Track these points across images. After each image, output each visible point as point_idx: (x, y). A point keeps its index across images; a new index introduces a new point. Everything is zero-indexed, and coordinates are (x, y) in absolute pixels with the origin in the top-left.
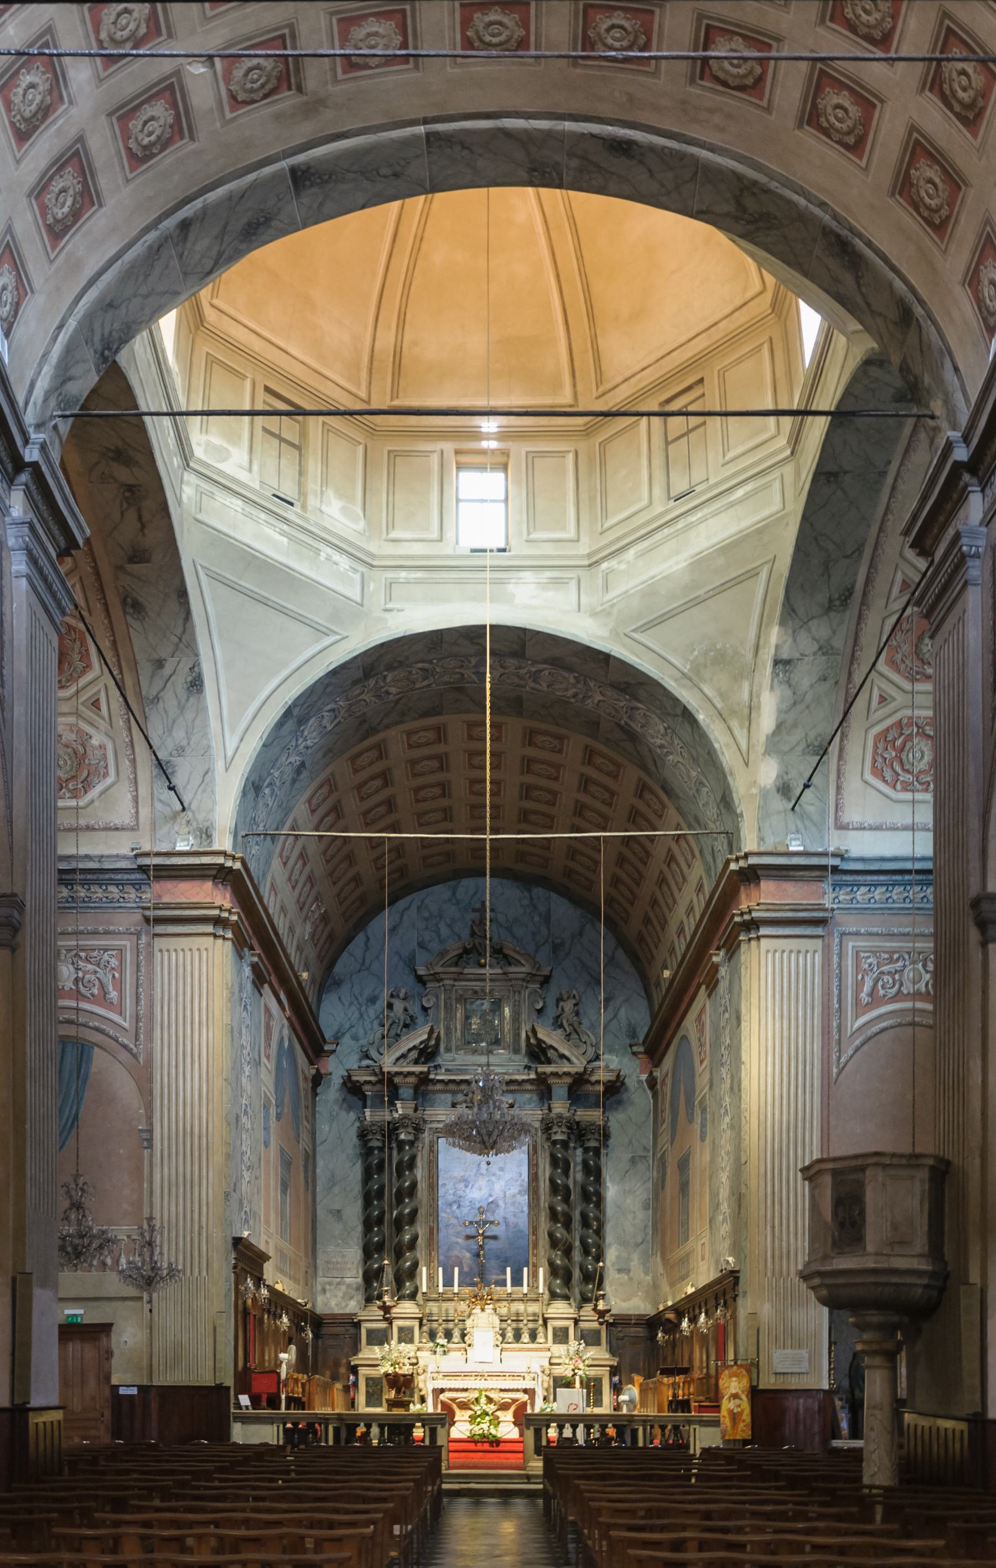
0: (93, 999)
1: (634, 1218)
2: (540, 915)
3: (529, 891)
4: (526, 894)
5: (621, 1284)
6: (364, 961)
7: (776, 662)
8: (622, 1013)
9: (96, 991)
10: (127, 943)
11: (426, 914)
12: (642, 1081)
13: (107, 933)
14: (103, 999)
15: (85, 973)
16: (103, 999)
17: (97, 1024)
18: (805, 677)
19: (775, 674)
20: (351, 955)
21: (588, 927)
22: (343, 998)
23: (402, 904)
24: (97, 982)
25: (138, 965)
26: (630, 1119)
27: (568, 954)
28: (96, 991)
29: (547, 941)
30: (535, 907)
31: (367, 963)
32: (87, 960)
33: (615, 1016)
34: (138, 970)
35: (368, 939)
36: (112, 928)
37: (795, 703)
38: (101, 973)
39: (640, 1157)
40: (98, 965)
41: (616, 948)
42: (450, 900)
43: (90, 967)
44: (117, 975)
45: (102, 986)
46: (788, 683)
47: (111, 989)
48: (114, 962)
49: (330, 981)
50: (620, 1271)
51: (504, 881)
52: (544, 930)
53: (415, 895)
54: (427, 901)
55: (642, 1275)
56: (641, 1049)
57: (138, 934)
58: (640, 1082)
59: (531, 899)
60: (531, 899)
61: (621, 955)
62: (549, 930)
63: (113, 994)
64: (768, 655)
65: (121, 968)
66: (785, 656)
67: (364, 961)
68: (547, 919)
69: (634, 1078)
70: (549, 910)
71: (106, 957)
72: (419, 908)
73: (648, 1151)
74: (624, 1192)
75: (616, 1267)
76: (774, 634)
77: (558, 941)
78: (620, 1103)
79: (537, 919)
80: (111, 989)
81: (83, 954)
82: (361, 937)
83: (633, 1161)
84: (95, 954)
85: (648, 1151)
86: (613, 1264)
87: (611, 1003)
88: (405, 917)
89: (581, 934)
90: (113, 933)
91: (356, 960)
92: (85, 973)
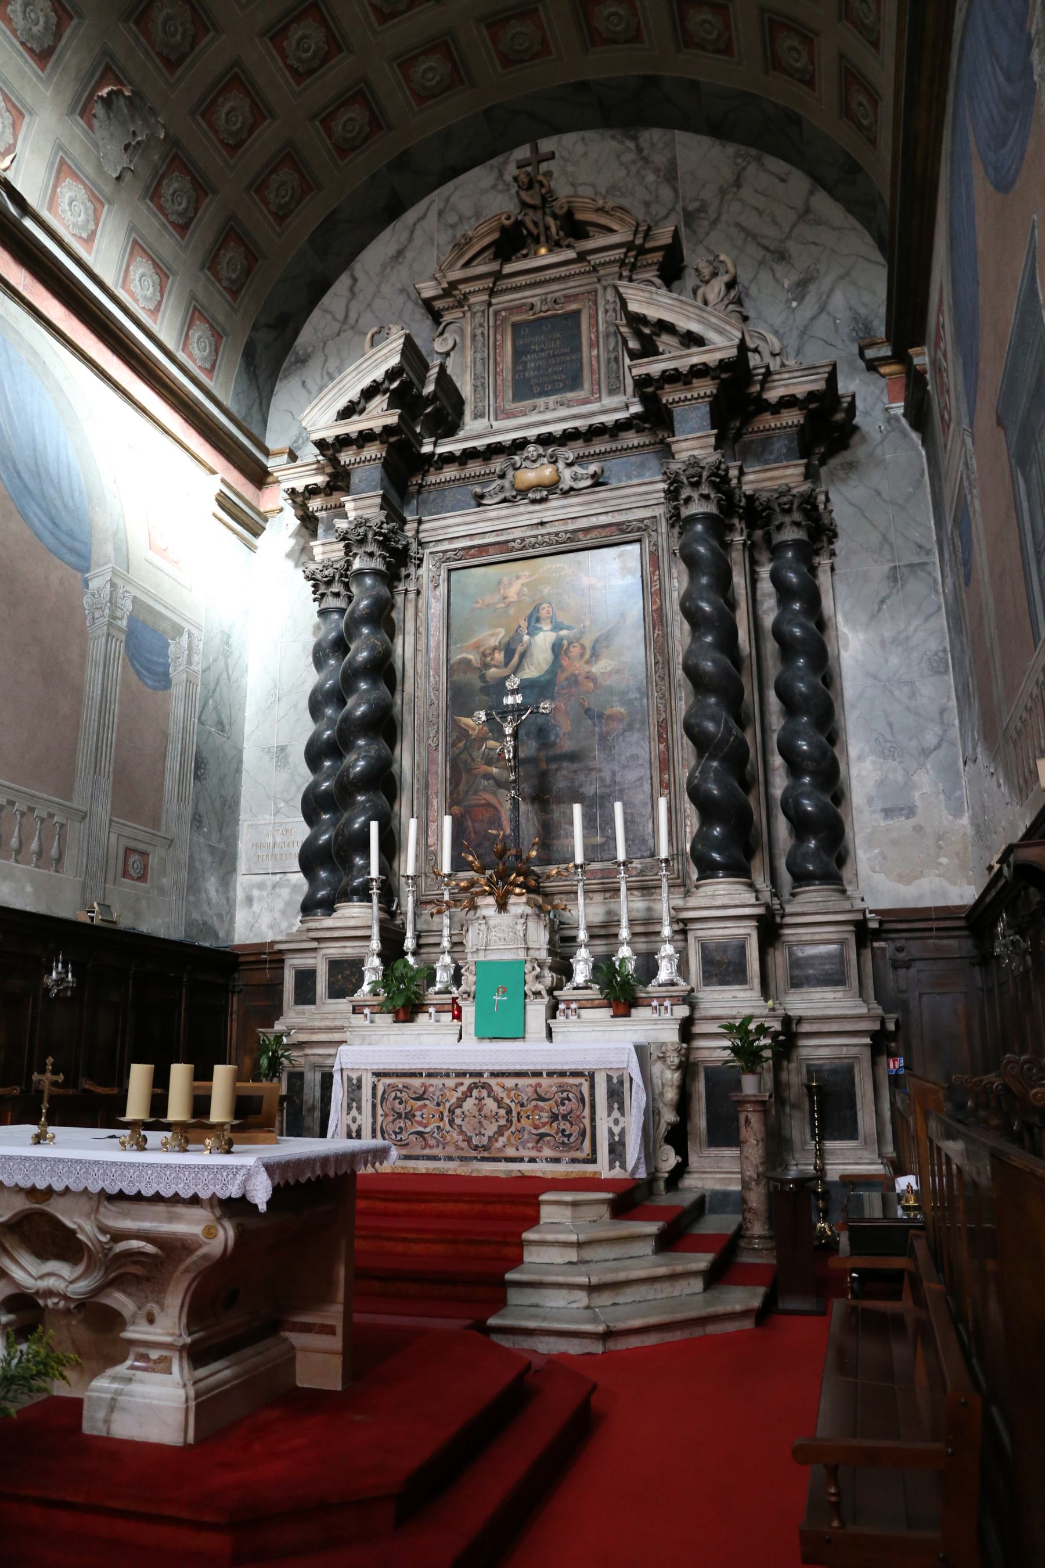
1: (913, 695)
2: (657, 171)
3: (635, 138)
4: (631, 145)
5: (894, 843)
6: (346, 317)
8: (838, 300)
11: (452, 218)
12: (896, 418)
20: (326, 311)
21: (752, 168)
22: (310, 383)
23: (410, 216)
26: (879, 494)
27: (717, 220)
29: (673, 209)
30: (646, 160)
31: (352, 320)
33: (822, 309)
35: (355, 280)
39: (911, 566)
41: (811, 193)
42: (494, 187)
49: (290, 358)
50: (888, 813)
51: (589, 134)
52: (666, 193)
53: (434, 195)
54: (453, 199)
55: (947, 818)
56: (886, 351)
58: (891, 420)
59: (639, 150)
60: (639, 150)
61: (823, 203)
62: (675, 190)
67: (346, 317)
68: (670, 176)
69: (878, 413)
70: (673, 162)
72: (440, 213)
73: (929, 552)
74: (883, 644)
75: (879, 805)
77: (693, 206)
78: (851, 466)
79: (651, 178)
82: (343, 282)
83: (894, 576)
85: (929, 552)
86: (870, 801)
87: (812, 288)
88: (418, 232)
89: (738, 184)
91: (335, 319)
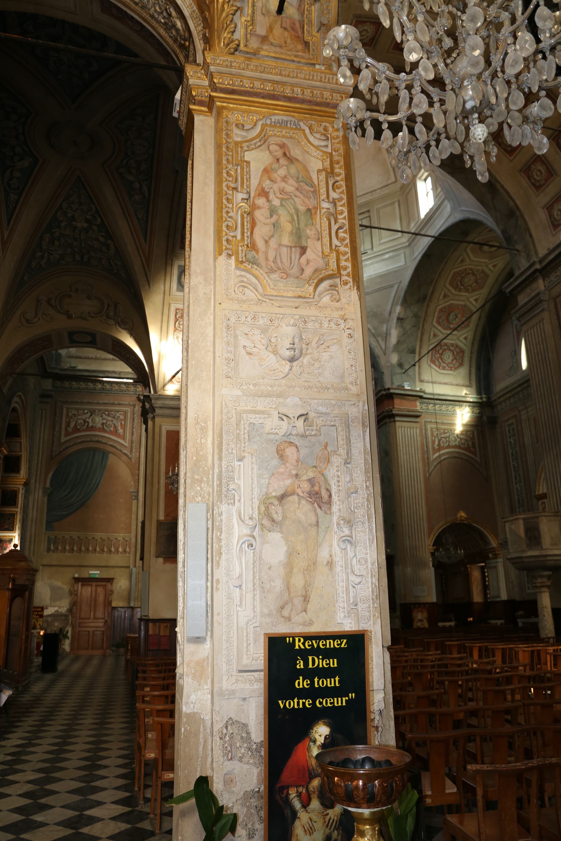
0: (111, 433)
7: (399, 319)
9: (112, 429)
10: (129, 409)
13: (119, 404)
14: (115, 433)
15: (107, 421)
16: (115, 433)
17: (112, 443)
18: (408, 325)
19: (397, 323)
24: (113, 425)
25: (133, 419)
28: (112, 429)
32: (108, 415)
34: (133, 421)
36: (121, 402)
37: (404, 334)
38: (115, 421)
40: (114, 418)
43: (110, 418)
44: (123, 423)
45: (115, 427)
46: (402, 326)
47: (119, 428)
48: (122, 417)
57: (134, 406)
63: (121, 431)
64: (395, 316)
65: (125, 419)
66: (401, 316)
71: (118, 414)
76: (398, 309)
80: (119, 428)
81: (107, 413)
84: (113, 413)
90: (122, 404)
92: (107, 421)
